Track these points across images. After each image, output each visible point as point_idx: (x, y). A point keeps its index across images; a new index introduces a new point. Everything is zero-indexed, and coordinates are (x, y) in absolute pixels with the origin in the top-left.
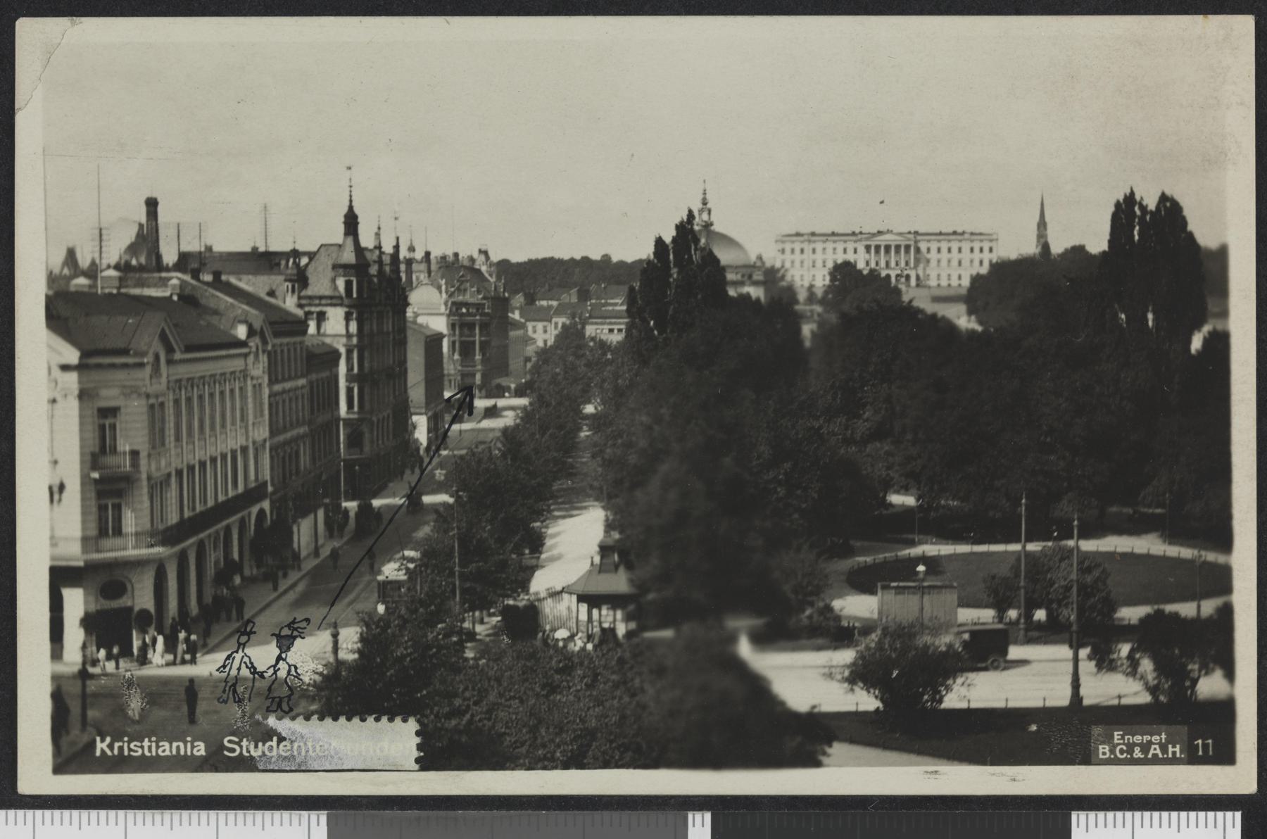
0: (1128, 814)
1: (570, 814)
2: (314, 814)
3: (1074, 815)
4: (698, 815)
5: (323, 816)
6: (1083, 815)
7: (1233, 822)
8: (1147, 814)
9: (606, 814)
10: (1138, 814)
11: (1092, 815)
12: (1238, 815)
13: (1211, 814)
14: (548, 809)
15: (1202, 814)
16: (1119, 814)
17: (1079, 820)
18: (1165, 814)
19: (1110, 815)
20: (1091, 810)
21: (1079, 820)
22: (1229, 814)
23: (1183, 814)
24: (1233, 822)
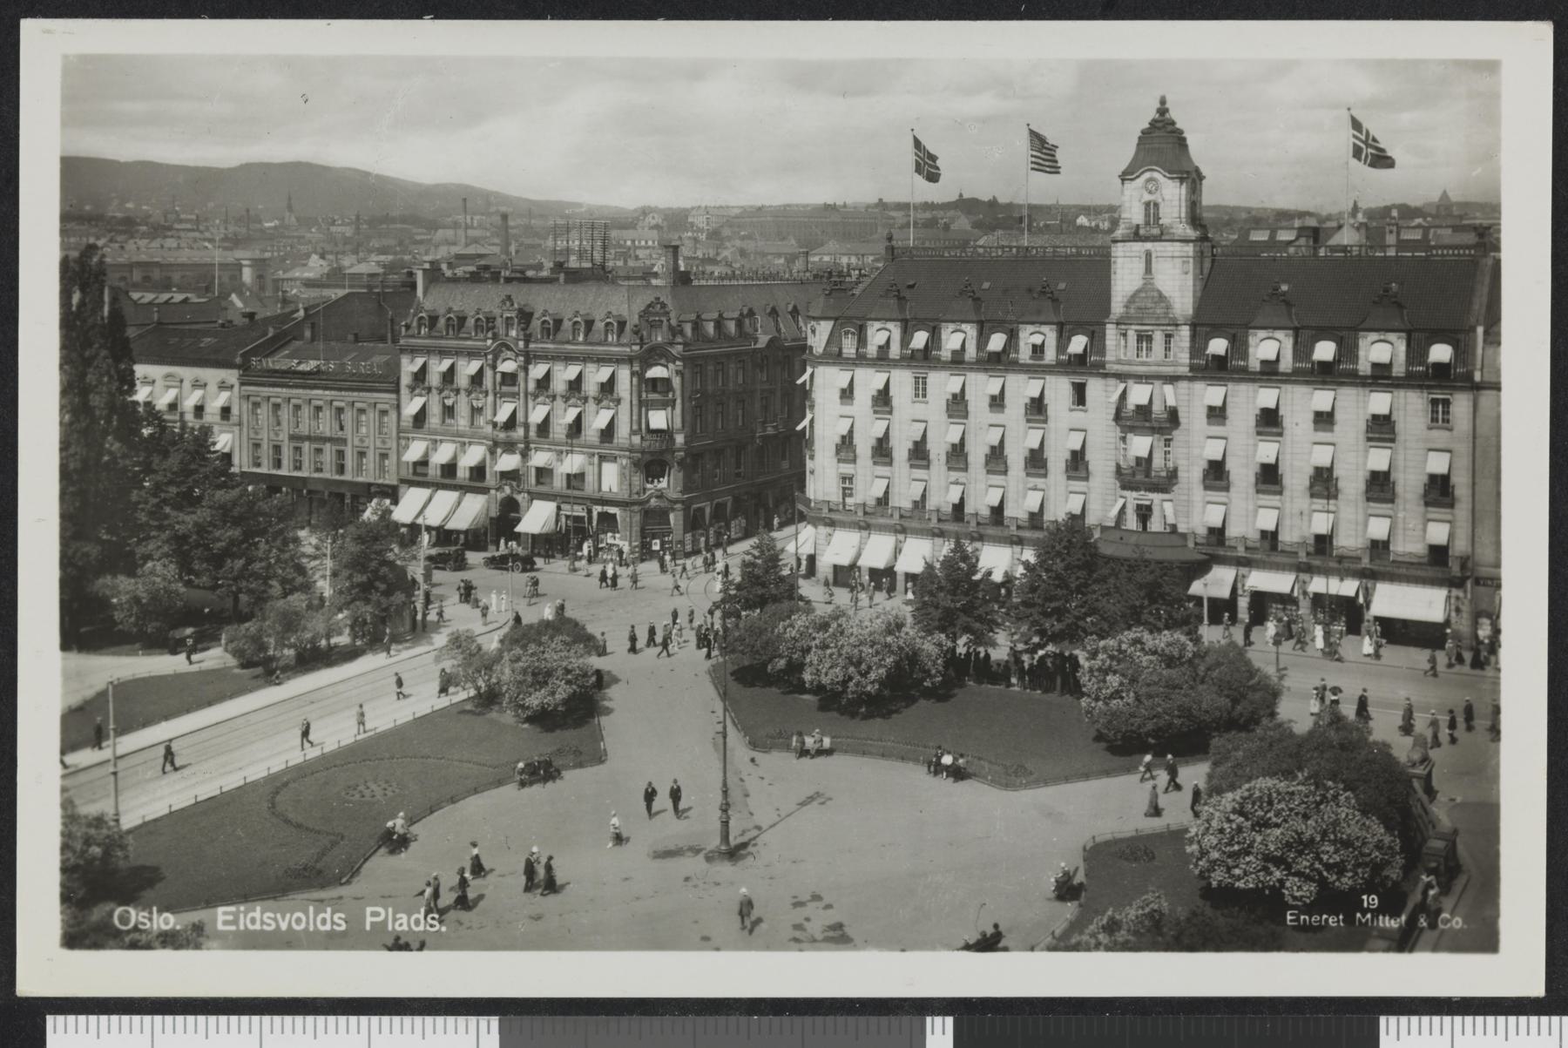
1: (786, 1020)
2: (483, 1020)
3: (1383, 1019)
4: (938, 1020)
5: (495, 1021)
6: (1393, 1019)
11: (1404, 1019)
14: (761, 1013)
17: (1388, 1026)
21: (1388, 1026)
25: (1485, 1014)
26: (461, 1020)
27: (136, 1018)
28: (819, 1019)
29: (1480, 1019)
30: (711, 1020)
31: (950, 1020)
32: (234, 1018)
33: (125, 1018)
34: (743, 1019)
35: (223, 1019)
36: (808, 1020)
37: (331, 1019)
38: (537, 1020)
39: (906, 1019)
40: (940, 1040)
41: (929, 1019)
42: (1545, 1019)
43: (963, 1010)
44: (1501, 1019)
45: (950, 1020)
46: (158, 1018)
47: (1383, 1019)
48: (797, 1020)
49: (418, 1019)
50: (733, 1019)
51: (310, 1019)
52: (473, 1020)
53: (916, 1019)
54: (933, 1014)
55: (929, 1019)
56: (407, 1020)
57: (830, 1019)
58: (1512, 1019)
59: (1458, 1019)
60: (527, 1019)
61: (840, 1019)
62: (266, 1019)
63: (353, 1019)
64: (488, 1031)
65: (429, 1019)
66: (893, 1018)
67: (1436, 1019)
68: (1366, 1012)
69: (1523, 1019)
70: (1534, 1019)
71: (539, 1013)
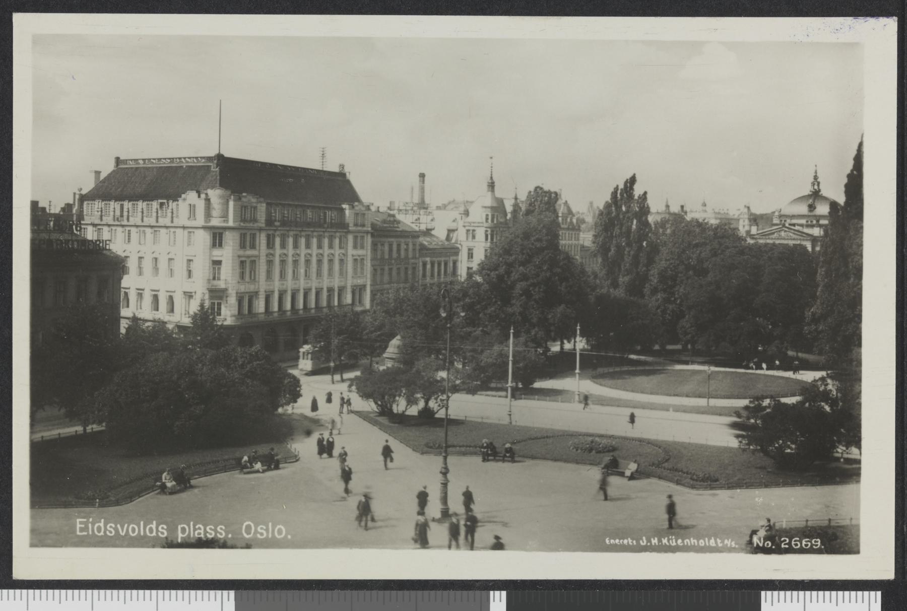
0: (801, 593)
2: (225, 592)
3: (763, 593)
4: (497, 593)
6: (769, 593)
7: (875, 599)
8: (814, 593)
12: (879, 593)
13: (860, 593)
14: (392, 589)
15: (853, 593)
17: (766, 597)
18: (827, 593)
19: (788, 593)
21: (766, 597)
22: (873, 593)
23: (840, 593)
25: (824, 590)
26: (212, 592)
28: (426, 593)
29: (821, 593)
30: (361, 593)
31: (504, 593)
33: (11, 591)
34: (381, 593)
35: (70, 592)
36: (420, 593)
37: (135, 592)
38: (258, 593)
39: (478, 592)
40: (498, 605)
41: (492, 592)
44: (834, 593)
45: (504, 593)
46: (31, 591)
47: (763, 593)
48: (413, 593)
49: (186, 592)
52: (219, 592)
56: (180, 592)
57: (433, 592)
59: (808, 593)
60: (251, 592)
61: (439, 593)
62: (96, 592)
63: (148, 592)
64: (228, 600)
65: (193, 592)
67: (795, 593)
68: (753, 589)
69: (847, 593)
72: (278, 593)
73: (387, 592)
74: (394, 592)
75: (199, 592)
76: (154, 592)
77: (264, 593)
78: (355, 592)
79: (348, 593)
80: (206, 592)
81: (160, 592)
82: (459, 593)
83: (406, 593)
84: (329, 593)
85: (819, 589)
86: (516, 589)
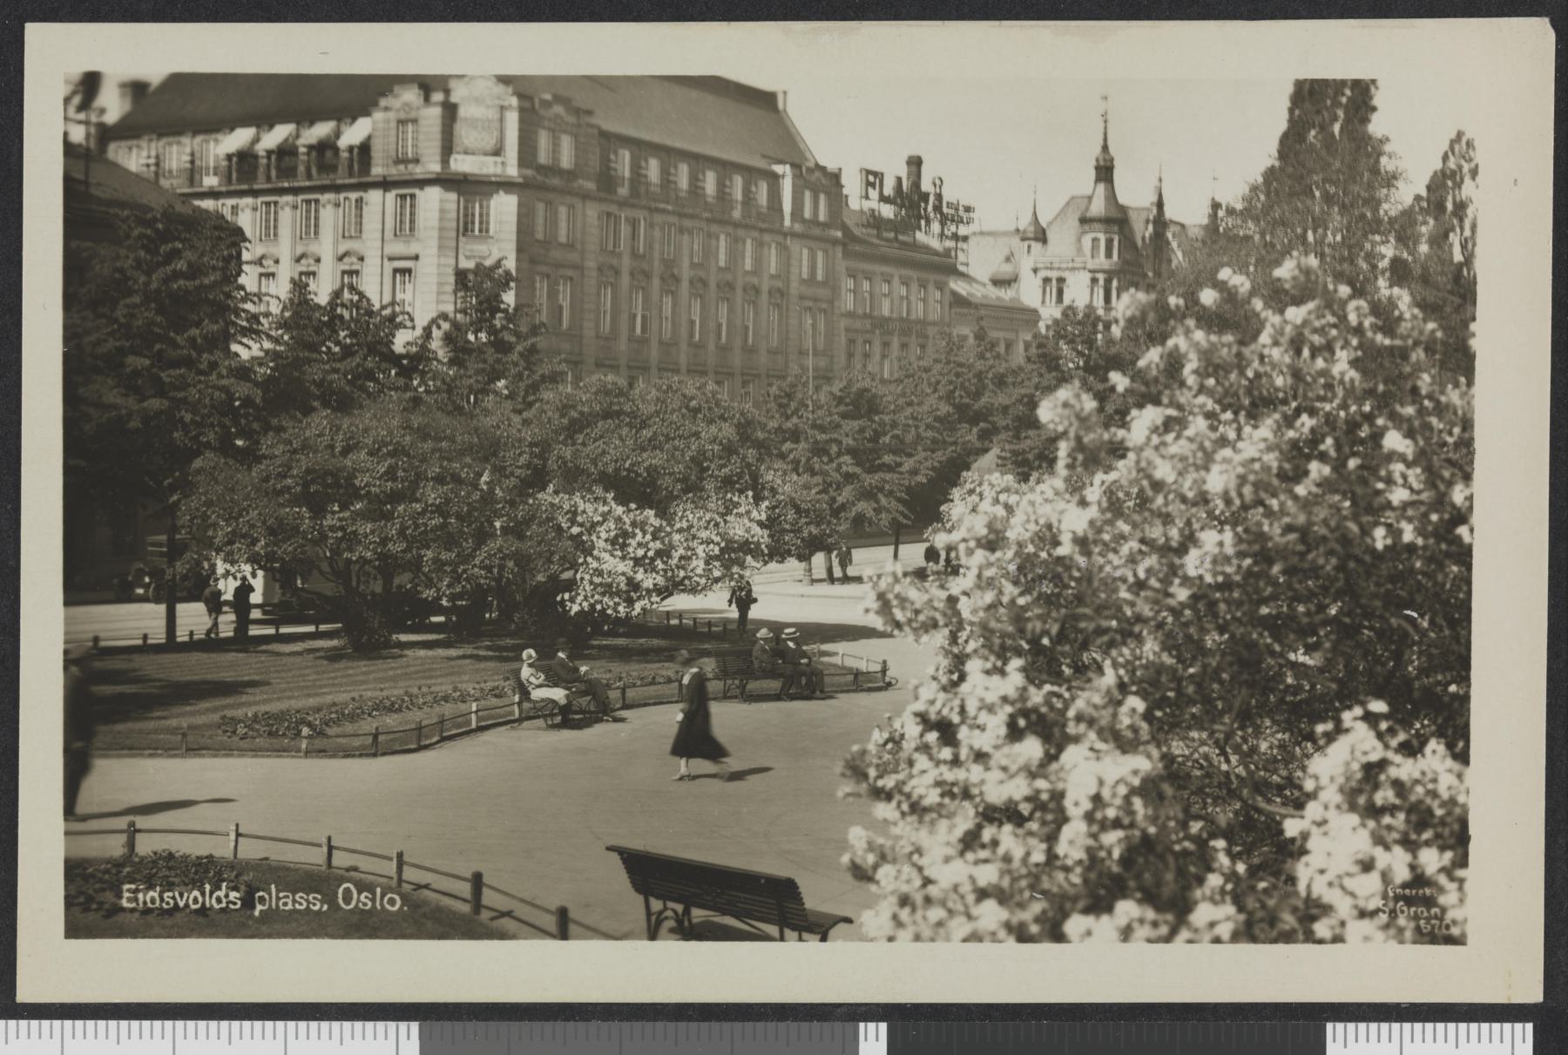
0: (1396, 1026)
2: (403, 1025)
3: (1329, 1026)
4: (872, 1026)
5: (415, 1027)
6: (1340, 1026)
7: (1522, 1037)
8: (1418, 1026)
9: (760, 1025)
10: (1407, 1026)
11: (1351, 1026)
12: (1530, 1027)
14: (690, 1019)
16: (1385, 1026)
17: (1336, 1033)
18: (1440, 1026)
20: (1350, 1021)
21: (1336, 1033)
22: (1519, 1026)
24: (1522, 1037)
25: (1435, 1020)
26: (381, 1025)
27: (46, 1023)
28: (749, 1025)
29: (1429, 1026)
30: (637, 1025)
31: (883, 1026)
32: (146, 1024)
34: (671, 1025)
35: (135, 1024)
36: (738, 1025)
37: (247, 1024)
38: (458, 1025)
39: (838, 1025)
41: (862, 1025)
42: (1496, 1026)
43: (895, 1015)
44: (1451, 1026)
45: (883, 1026)
47: (1329, 1026)
48: (726, 1026)
49: (336, 1025)
50: (660, 1025)
51: (224, 1024)
52: (392, 1025)
53: (849, 1025)
54: (866, 1020)
55: (862, 1025)
56: (325, 1025)
58: (1462, 1026)
60: (447, 1025)
61: (771, 1025)
62: (180, 1024)
65: (347, 1025)
66: (825, 1024)
68: (1310, 1019)
69: (1474, 1026)
70: (1485, 1026)
71: (459, 1019)
72: (493, 1025)
73: (682, 1025)
74: (693, 1025)
75: (358, 1025)
76: (280, 1024)
77: (471, 1026)
78: (626, 1025)
79: (615, 1025)
80: (370, 1025)
81: (291, 1024)
82: (805, 1025)
83: (715, 1025)
84: (581, 1025)
85: (1425, 1020)
86: (902, 1018)
